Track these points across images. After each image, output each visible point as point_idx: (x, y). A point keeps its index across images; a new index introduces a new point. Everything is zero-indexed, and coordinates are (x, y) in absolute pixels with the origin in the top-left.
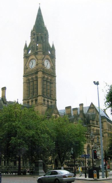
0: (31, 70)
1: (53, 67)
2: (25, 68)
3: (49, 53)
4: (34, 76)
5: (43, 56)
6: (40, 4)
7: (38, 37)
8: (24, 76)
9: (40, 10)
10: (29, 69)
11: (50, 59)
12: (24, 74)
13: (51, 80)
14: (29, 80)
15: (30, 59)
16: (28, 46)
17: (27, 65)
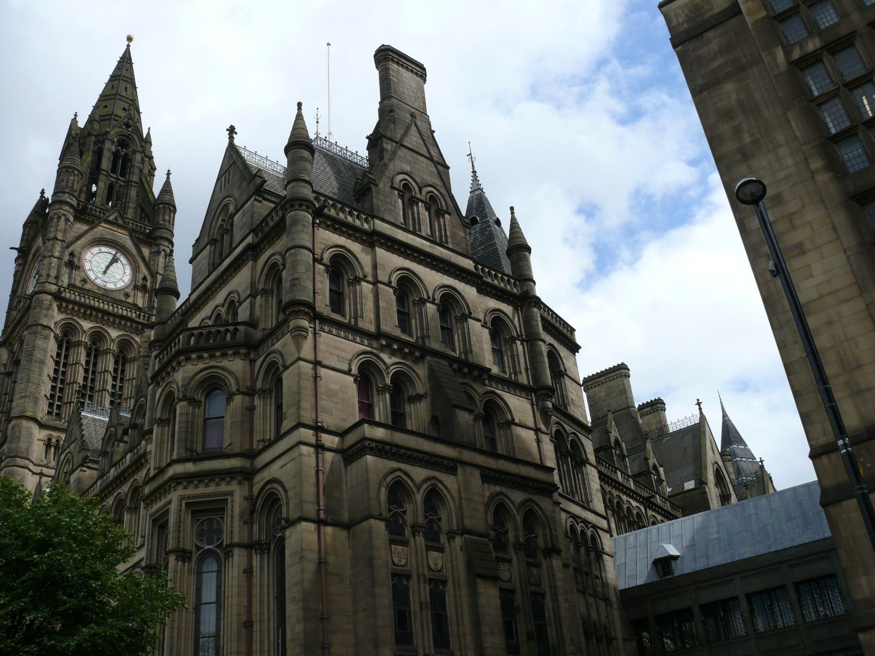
1: (145, 279)
6: (130, 39)
9: (126, 61)
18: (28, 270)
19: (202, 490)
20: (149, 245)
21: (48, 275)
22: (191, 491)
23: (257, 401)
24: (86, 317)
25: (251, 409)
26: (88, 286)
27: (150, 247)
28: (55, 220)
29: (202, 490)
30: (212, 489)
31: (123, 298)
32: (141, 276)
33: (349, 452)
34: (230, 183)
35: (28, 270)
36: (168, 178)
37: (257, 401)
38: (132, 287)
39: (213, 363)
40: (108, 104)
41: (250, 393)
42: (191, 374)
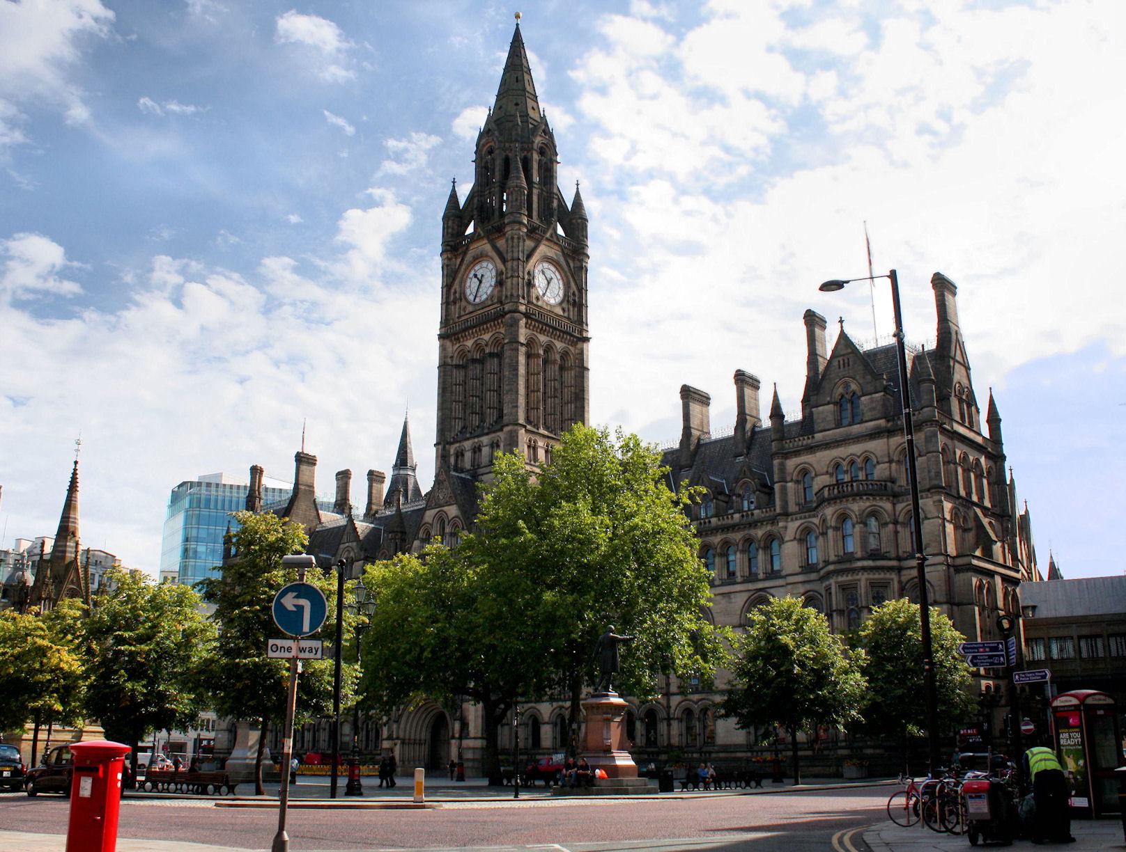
0: (470, 308)
1: (574, 294)
2: (448, 297)
3: (560, 231)
4: (487, 337)
5: (529, 244)
7: (507, 162)
8: (441, 337)
10: (464, 303)
11: (562, 260)
12: (445, 322)
13: (565, 355)
14: (462, 353)
15: (468, 258)
16: (462, 201)
17: (456, 286)
18: (465, 270)
19: (877, 576)
20: (574, 259)
21: (518, 296)
22: (871, 576)
23: (899, 528)
24: (542, 332)
25: (896, 532)
26: (540, 303)
27: (574, 261)
28: (516, 240)
29: (877, 576)
30: (882, 576)
31: (561, 313)
32: (572, 291)
33: (960, 568)
34: (850, 367)
35: (465, 270)
36: (578, 188)
37: (899, 528)
38: (566, 302)
39: (874, 503)
40: (519, 102)
41: (896, 522)
42: (864, 508)
